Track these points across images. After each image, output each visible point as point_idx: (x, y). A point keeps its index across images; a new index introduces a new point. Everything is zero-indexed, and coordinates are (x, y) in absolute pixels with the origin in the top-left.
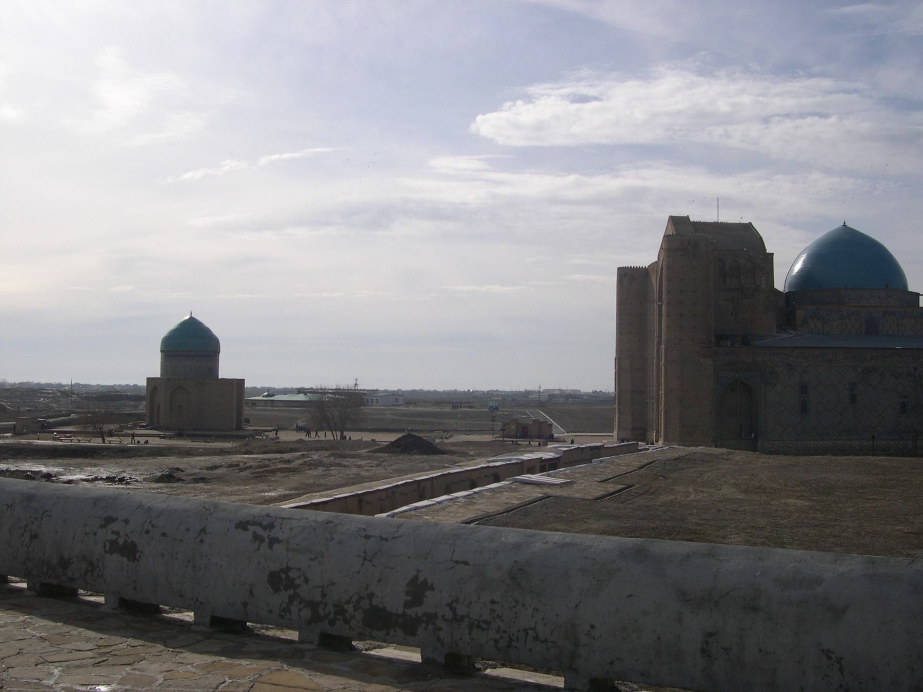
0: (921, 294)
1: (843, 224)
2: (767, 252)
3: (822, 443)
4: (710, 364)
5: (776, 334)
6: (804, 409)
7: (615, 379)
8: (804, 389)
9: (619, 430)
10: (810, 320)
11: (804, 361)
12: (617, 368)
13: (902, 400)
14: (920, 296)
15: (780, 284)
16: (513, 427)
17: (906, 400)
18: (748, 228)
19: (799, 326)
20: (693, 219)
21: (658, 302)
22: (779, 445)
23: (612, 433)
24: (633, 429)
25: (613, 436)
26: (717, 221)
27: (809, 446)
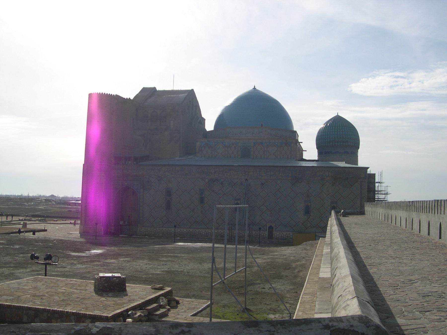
1: (254, 88)
3: (180, 230)
4: (103, 176)
6: (168, 206)
8: (169, 193)
15: (210, 126)
18: (144, 88)
22: (151, 231)
26: (172, 89)
27: (171, 231)
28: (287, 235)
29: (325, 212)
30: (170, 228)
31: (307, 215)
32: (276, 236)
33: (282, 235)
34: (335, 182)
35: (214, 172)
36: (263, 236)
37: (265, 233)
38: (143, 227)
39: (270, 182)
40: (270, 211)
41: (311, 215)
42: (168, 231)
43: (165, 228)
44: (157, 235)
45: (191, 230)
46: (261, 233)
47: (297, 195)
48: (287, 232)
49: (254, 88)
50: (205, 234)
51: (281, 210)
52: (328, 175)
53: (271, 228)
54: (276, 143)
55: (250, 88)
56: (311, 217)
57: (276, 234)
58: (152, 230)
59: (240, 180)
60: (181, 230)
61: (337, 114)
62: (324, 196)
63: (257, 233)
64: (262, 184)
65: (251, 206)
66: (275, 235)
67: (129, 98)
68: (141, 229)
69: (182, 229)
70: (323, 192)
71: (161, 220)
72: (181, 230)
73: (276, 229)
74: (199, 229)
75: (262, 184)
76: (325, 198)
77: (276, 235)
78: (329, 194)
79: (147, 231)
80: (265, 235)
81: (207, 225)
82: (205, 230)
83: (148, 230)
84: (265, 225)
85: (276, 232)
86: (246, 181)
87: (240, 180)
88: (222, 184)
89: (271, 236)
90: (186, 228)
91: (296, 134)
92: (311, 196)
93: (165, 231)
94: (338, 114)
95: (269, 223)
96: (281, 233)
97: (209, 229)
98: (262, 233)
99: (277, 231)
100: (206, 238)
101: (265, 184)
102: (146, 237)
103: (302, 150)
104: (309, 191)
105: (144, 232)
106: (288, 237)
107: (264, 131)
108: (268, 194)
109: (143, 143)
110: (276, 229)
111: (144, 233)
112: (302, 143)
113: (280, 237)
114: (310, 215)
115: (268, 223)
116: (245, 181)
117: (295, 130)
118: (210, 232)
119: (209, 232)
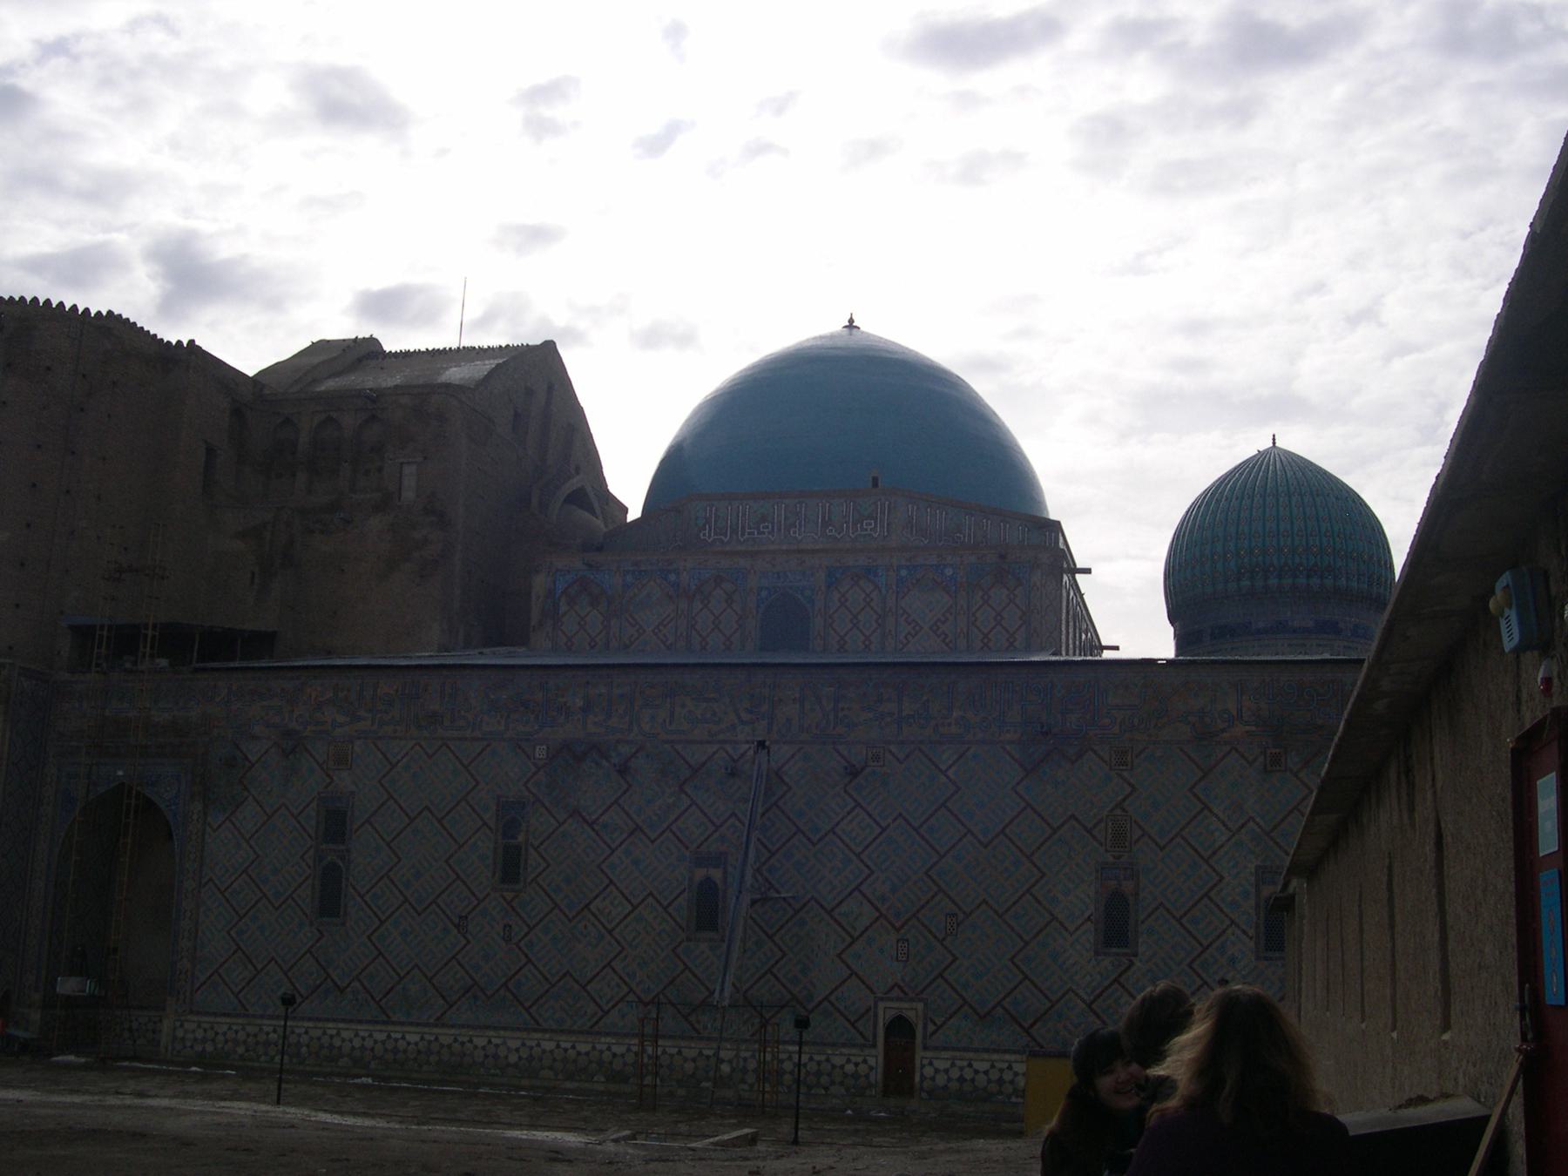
1: (848, 324)
10: (563, 608)
11: (341, 719)
13: (700, 874)
17: (716, 874)
27: (337, 1042)
28: (994, 1075)
29: (1224, 931)
30: (330, 1025)
31: (1114, 950)
32: (933, 1079)
33: (968, 1074)
34: (1278, 751)
35: (580, 703)
36: (855, 1076)
37: (865, 1061)
38: (191, 1012)
39: (893, 754)
40: (898, 930)
42: (319, 1039)
43: (306, 1024)
44: (263, 1058)
46: (805, 1058)
47: (1055, 831)
48: (995, 1057)
49: (848, 324)
50: (520, 1058)
51: (958, 925)
52: (1235, 713)
53: (900, 1028)
54: (948, 572)
55: (835, 325)
56: (1138, 964)
57: (931, 1064)
58: (237, 1032)
59: (729, 748)
60: (389, 1037)
61: (1271, 445)
62: (1217, 834)
63: (817, 1058)
64: (853, 772)
65: (784, 899)
66: (922, 1075)
67: (192, 342)
68: (182, 1026)
69: (398, 1028)
70: (1206, 812)
71: (286, 974)
72: (389, 1037)
73: (934, 1033)
74: (492, 1033)
75: (853, 772)
76: (1222, 846)
77: (929, 1071)
78: (1243, 826)
79: (210, 1034)
80: (863, 1069)
81: (535, 1008)
82: (524, 1035)
83: (217, 1034)
84: (868, 1011)
85: (929, 1054)
86: (756, 753)
87: (729, 748)
88: (623, 770)
89: (898, 1076)
90: (418, 1025)
91: (1060, 535)
92: (1138, 840)
93: (304, 1039)
94: (1274, 443)
95: (891, 1000)
96: (959, 1063)
97: (545, 1031)
98: (849, 1061)
99: (936, 1048)
100: (525, 1082)
101: (868, 770)
102: (194, 1069)
103: (1097, 644)
104: (1124, 810)
105: (195, 1039)
106: (1000, 1081)
107: (883, 512)
108: (884, 830)
109: (253, 574)
110: (934, 1033)
111: (192, 1047)
112: (1088, 571)
113: (954, 1085)
114: (1136, 955)
115: (882, 999)
116: (751, 752)
117: (1053, 516)
118: (551, 1052)
119: (544, 1051)
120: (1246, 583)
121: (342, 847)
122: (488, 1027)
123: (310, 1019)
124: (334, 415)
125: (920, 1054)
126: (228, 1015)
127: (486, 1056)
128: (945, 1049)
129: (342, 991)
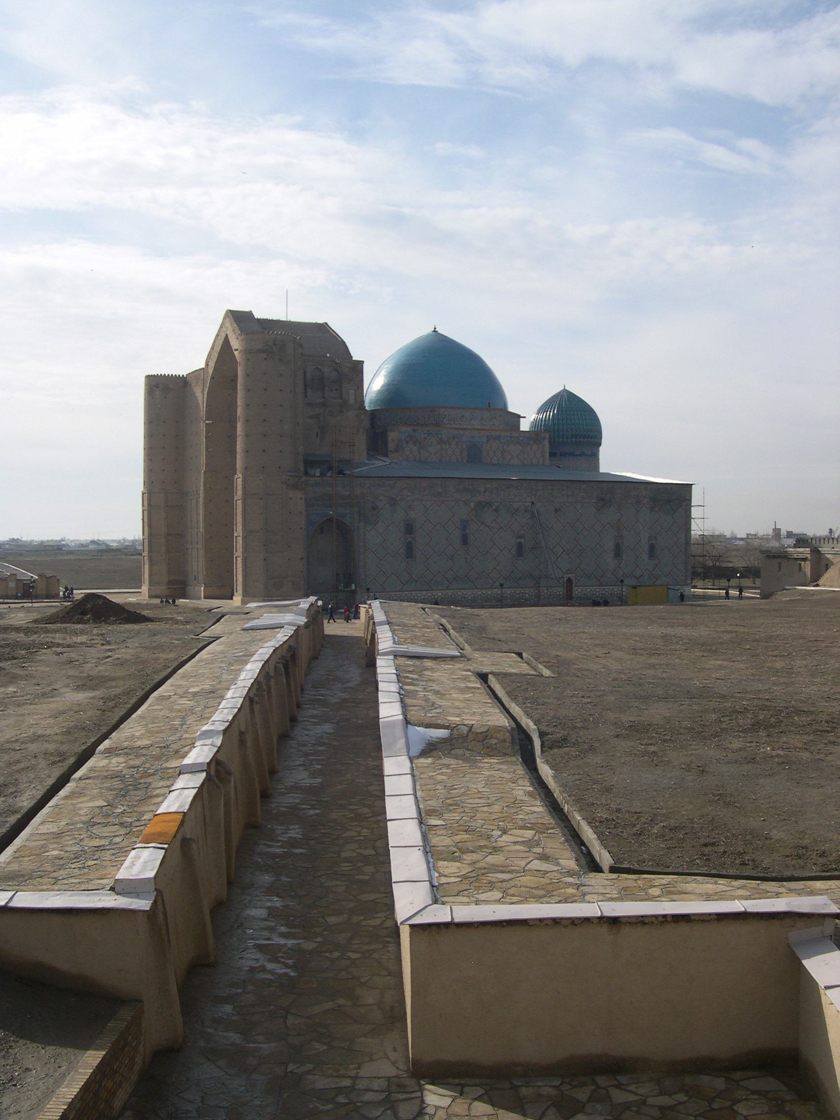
0: (522, 416)
1: (433, 330)
2: (354, 359)
5: (367, 461)
6: (410, 551)
7: (143, 519)
8: (409, 529)
9: (151, 583)
10: (405, 445)
12: (146, 504)
14: (521, 419)
16: (12, 585)
17: (522, 540)
19: (391, 451)
20: (258, 315)
21: (206, 420)
23: (141, 588)
24: (169, 582)
25: (141, 592)
35: (483, 490)
41: (624, 558)
45: (450, 592)
53: (569, 581)
55: (427, 330)
64: (556, 511)
75: (556, 511)
77: (577, 592)
85: (576, 588)
88: (496, 510)
109: (317, 433)
120: (574, 439)
121: (412, 536)
122: (461, 589)
123: (407, 591)
124: (319, 367)
125: (574, 588)
126: (380, 592)
127: (462, 598)
128: (580, 586)
129: (416, 581)
